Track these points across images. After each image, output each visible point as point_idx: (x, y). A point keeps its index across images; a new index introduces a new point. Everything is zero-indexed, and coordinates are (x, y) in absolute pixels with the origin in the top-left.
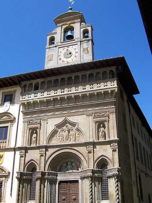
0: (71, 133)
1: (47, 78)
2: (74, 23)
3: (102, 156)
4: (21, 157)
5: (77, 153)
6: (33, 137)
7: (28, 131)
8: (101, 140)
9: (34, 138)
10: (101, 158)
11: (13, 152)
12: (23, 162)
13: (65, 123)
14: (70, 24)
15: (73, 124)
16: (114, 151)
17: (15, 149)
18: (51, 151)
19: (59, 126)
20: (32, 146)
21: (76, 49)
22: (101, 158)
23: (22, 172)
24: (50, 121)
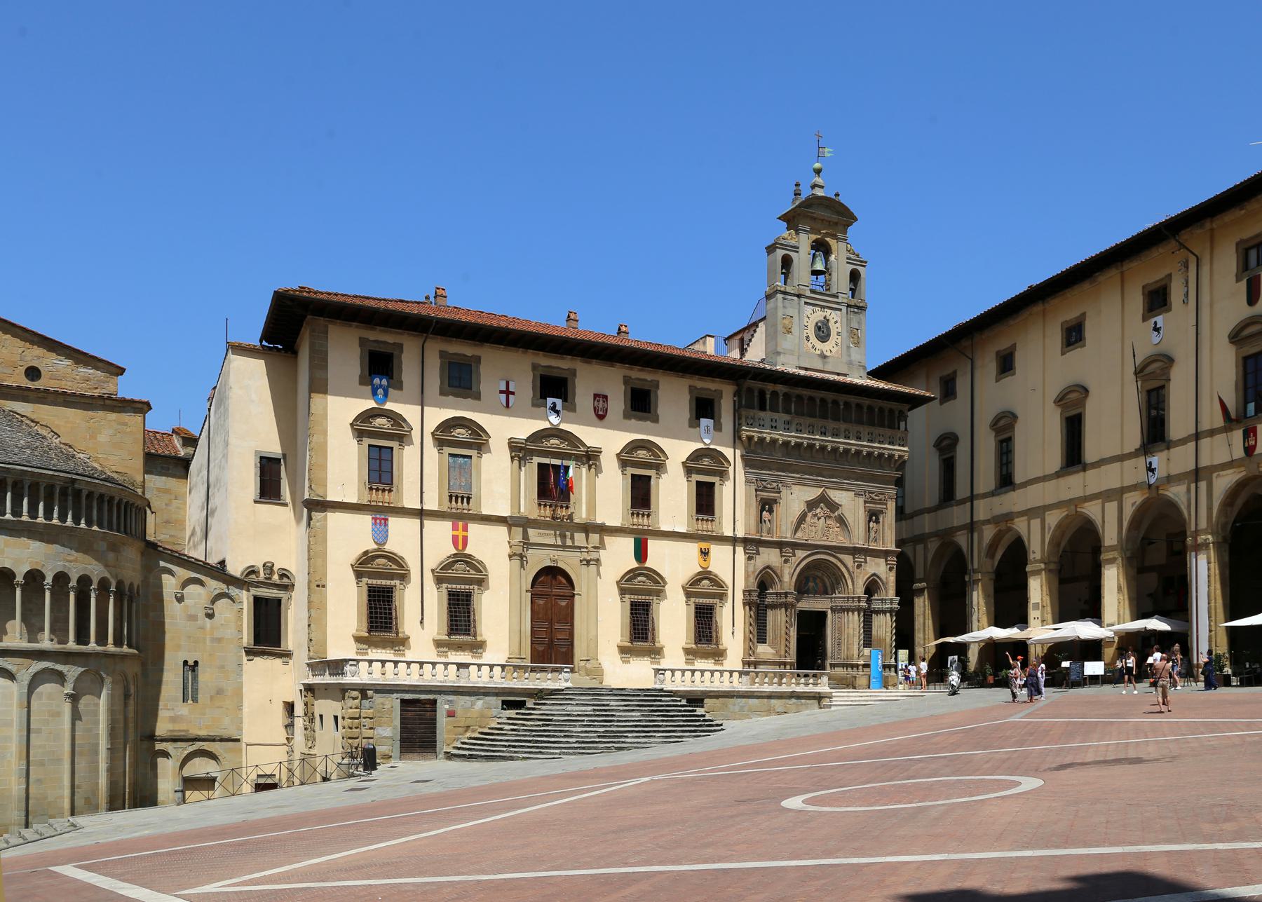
3: (874, 574)
5: (839, 564)
12: (751, 569)
13: (823, 500)
15: (833, 506)
16: (891, 569)
17: (734, 541)
18: (801, 554)
19: (811, 505)
24: (796, 489)
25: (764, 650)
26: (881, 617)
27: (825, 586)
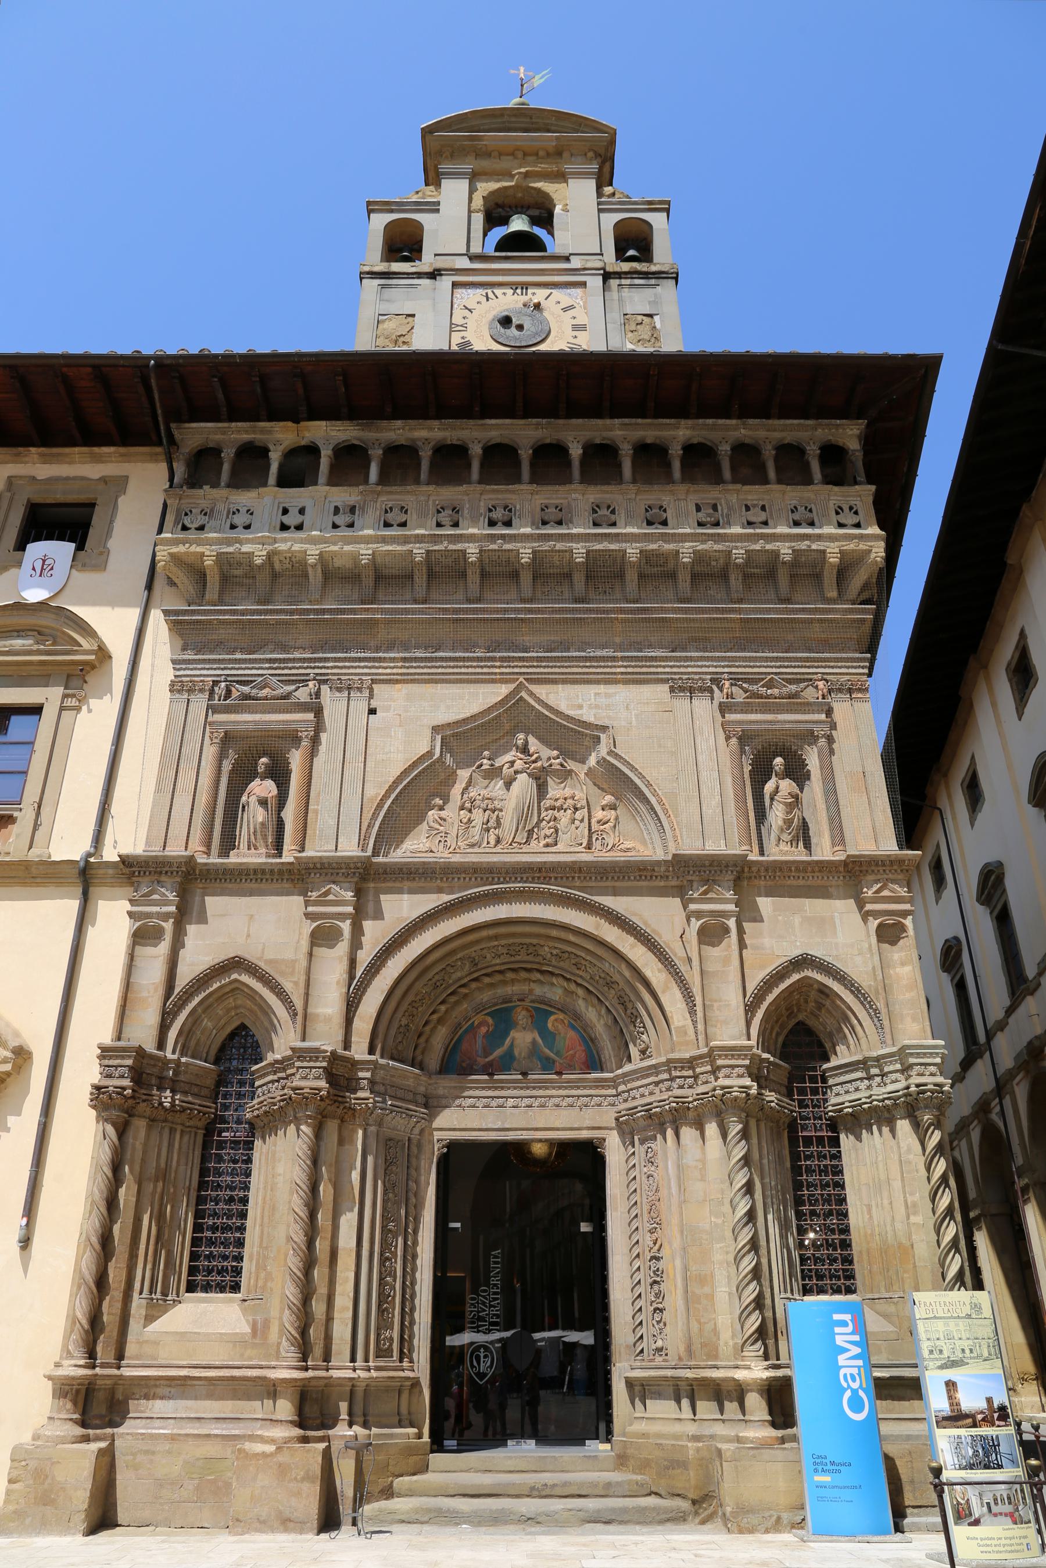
0: (555, 791)
1: (384, 423)
2: (561, 177)
4: (143, 935)
5: (611, 934)
6: (253, 799)
7: (211, 751)
8: (786, 853)
9: (263, 802)
10: (795, 977)
11: (72, 905)
13: (510, 722)
14: (527, 175)
15: (573, 738)
17: (86, 878)
18: (401, 907)
20: (243, 856)
21: (572, 307)
22: (795, 977)
23: (150, 1047)
24: (393, 699)
25: (198, 1327)
26: (876, 1140)
27: (589, 1042)
